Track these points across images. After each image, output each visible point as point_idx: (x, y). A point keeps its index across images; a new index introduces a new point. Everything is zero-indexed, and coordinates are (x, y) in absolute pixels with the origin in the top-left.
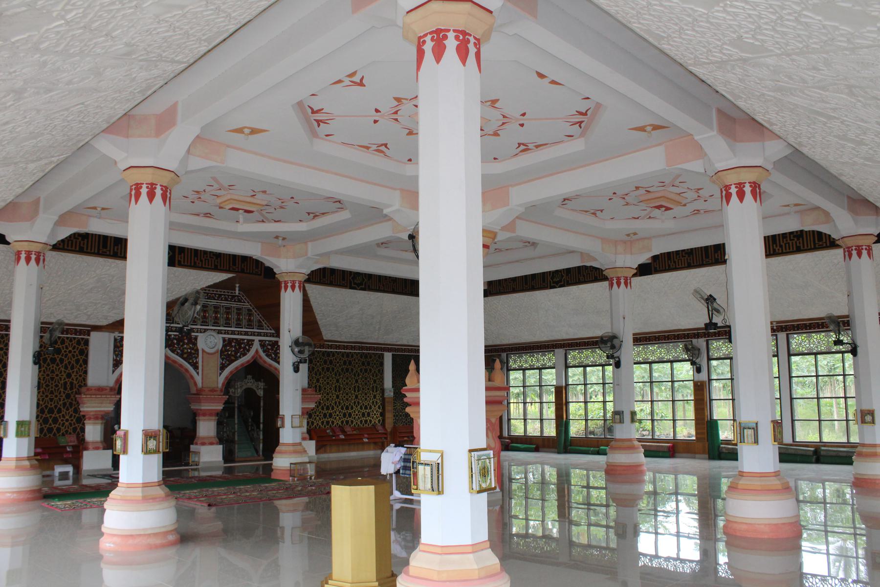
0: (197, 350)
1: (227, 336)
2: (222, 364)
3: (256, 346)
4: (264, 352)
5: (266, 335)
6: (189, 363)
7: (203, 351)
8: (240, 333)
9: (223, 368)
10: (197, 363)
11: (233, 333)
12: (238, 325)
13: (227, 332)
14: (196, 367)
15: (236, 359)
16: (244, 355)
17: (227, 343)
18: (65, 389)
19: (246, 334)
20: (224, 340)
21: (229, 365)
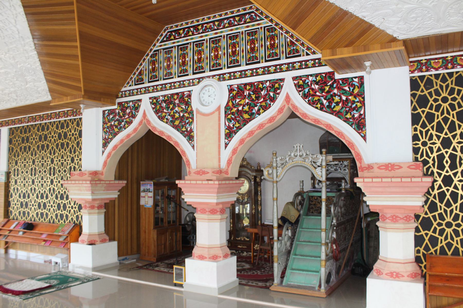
0: (191, 112)
1: (235, 82)
2: (229, 128)
3: (289, 88)
4: (305, 96)
5: (304, 65)
6: (182, 133)
7: (198, 112)
8: (255, 73)
9: (230, 134)
10: (191, 131)
11: (243, 74)
12: (252, 60)
13: (232, 76)
14: (189, 136)
15: (252, 116)
16: (266, 108)
17: (236, 93)
18: (441, 167)
19: (266, 71)
20: (231, 90)
21: (239, 128)
